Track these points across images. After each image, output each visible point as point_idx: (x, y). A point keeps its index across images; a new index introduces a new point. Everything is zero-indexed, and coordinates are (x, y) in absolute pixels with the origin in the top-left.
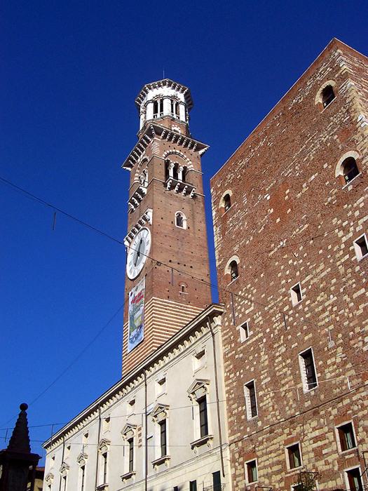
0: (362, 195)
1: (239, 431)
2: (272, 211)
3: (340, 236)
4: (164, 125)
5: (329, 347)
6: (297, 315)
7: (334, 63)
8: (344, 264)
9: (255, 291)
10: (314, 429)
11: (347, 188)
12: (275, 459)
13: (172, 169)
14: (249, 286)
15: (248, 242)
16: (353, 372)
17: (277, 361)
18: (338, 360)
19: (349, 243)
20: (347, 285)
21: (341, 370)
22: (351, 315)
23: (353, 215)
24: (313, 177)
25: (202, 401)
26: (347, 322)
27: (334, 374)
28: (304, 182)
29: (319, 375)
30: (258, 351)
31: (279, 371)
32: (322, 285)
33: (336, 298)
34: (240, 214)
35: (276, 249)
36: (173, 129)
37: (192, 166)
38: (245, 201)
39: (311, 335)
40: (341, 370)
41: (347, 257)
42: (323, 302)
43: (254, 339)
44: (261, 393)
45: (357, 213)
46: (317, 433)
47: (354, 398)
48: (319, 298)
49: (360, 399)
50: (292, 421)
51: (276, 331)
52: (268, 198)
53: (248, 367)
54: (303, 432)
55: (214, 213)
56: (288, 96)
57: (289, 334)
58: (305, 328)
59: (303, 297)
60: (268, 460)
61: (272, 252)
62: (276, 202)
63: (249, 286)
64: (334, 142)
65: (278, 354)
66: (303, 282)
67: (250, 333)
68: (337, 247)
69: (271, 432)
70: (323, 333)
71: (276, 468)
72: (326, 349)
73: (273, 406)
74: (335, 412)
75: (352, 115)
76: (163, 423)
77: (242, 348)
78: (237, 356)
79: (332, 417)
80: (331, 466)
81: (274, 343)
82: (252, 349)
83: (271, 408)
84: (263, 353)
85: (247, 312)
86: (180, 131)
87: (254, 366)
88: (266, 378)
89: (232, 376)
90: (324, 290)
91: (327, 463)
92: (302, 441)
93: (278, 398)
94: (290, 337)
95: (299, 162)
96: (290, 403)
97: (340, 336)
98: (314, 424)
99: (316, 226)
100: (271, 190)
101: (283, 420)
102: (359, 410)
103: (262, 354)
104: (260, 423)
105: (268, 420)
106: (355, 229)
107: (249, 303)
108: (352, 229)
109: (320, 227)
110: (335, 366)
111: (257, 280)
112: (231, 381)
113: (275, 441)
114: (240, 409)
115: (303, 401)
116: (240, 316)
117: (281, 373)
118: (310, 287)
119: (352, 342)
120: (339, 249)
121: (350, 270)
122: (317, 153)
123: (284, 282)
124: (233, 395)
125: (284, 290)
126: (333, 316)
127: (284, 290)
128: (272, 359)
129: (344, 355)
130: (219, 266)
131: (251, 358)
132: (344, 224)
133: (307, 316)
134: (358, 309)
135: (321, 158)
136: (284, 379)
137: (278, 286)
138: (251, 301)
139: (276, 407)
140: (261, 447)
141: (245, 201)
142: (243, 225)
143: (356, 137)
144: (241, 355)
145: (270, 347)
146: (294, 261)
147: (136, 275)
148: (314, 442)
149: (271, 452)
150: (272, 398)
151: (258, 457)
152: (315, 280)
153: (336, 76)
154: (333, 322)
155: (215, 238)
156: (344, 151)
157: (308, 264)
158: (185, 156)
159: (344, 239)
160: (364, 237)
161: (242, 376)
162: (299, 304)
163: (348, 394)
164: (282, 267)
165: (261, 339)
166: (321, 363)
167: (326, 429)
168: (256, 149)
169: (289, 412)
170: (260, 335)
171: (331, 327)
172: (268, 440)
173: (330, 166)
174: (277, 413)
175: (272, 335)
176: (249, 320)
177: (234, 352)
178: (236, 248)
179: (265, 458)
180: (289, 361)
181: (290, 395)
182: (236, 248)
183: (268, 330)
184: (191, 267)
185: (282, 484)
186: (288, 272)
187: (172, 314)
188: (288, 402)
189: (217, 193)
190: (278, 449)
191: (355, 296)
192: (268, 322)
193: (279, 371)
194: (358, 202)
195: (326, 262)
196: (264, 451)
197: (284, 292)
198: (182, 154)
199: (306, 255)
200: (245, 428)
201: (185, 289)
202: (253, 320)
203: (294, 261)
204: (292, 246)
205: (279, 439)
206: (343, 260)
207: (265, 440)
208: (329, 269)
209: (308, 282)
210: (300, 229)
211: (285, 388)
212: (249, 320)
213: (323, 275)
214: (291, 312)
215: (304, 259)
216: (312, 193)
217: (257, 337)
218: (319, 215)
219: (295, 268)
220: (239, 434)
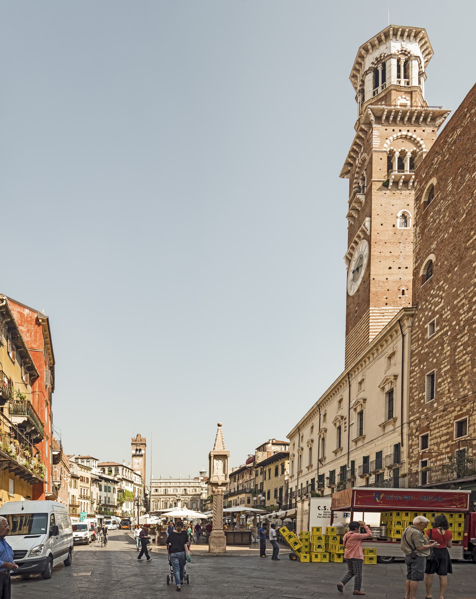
43: (440, 334)
84: (447, 344)
85: (436, 309)
93: (454, 382)
96: (465, 386)
101: (456, 400)
103: (445, 346)
113: (446, 418)
136: (462, 365)
139: (451, 390)
149: (442, 426)
170: (445, 329)
174: (452, 395)
176: (437, 316)
196: (437, 426)
202: (441, 315)
211: (462, 373)
217: (442, 332)
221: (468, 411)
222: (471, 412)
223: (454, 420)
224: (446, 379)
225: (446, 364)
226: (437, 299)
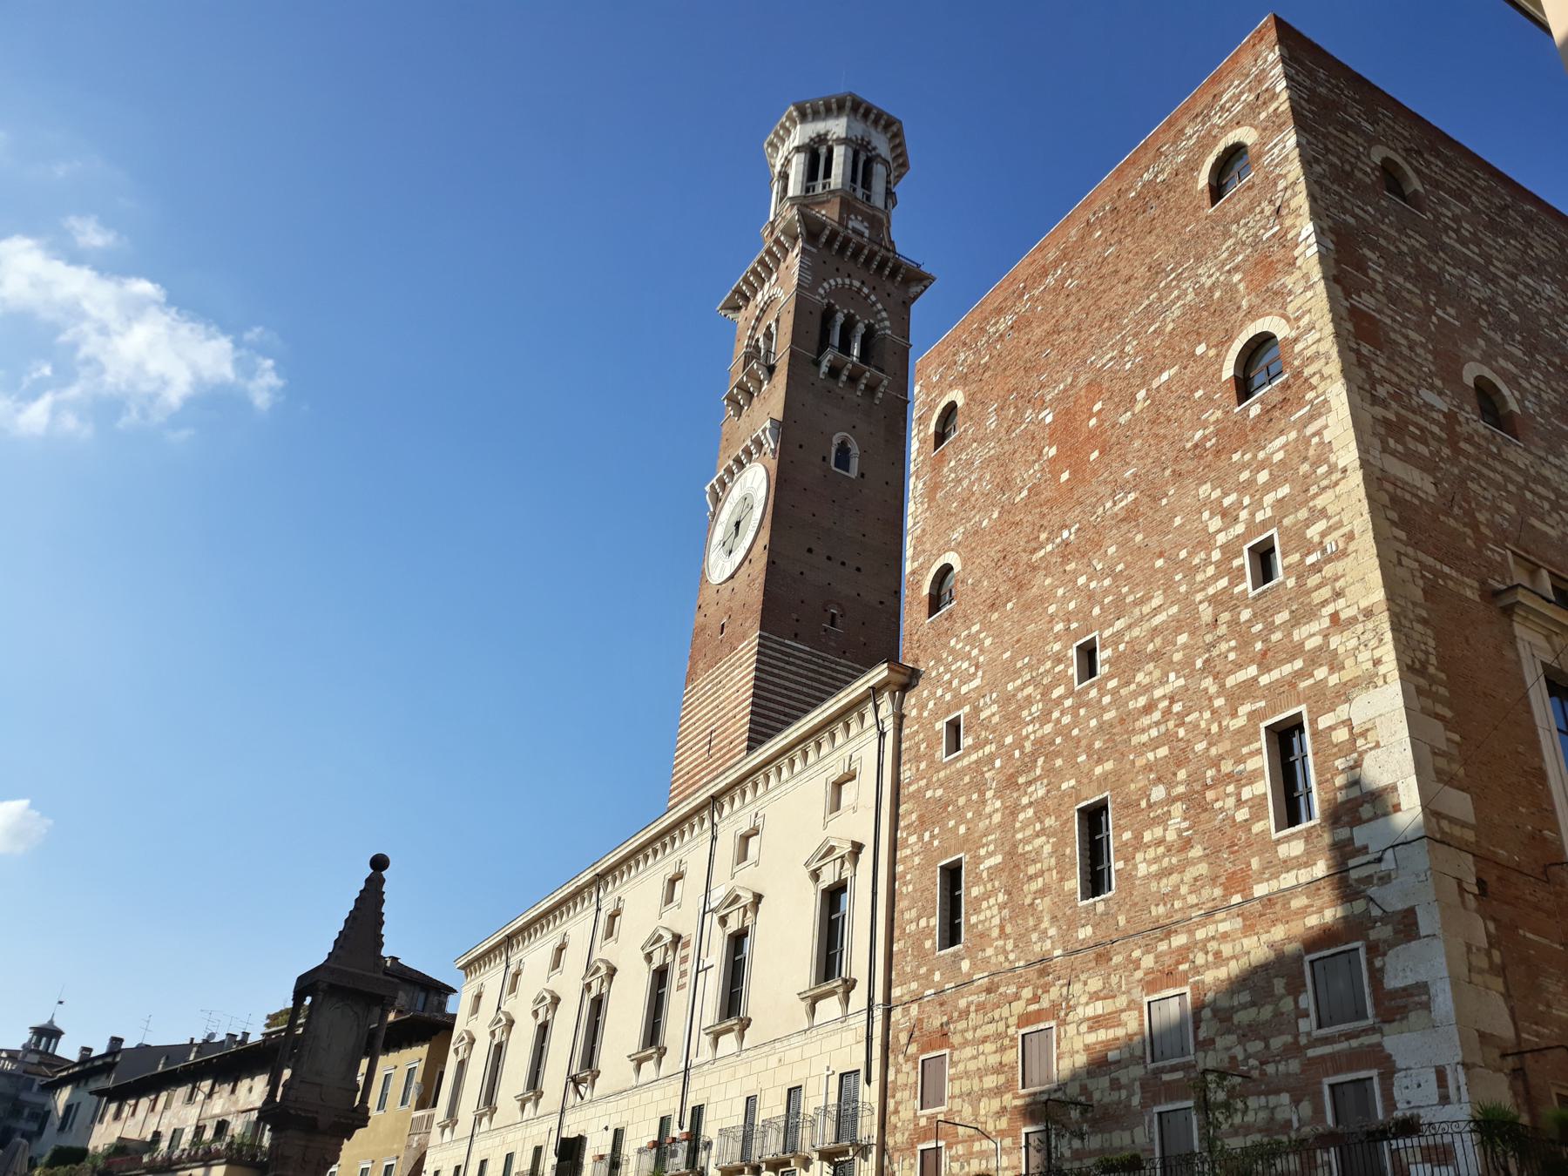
0: (1282, 432)
1: (916, 977)
2: (1053, 451)
3: (1211, 530)
4: (829, 213)
5: (1153, 798)
6: (1082, 712)
7: (1260, 82)
8: (1212, 600)
9: (988, 642)
10: (1095, 997)
11: (1247, 409)
12: (993, 1060)
13: (838, 329)
14: (975, 628)
15: (985, 523)
16: (1203, 868)
17: (1021, 817)
18: (1171, 836)
19: (1230, 551)
20: (1215, 652)
21: (1174, 860)
22: (1215, 728)
23: (1251, 482)
24: (1165, 376)
25: (833, 897)
26: (1204, 745)
27: (1154, 868)
28: (1140, 387)
29: (1120, 865)
30: (981, 787)
31: (1026, 841)
32: (1151, 647)
33: (1182, 682)
34: (979, 453)
35: (1049, 548)
36: (851, 224)
37: (887, 323)
38: (992, 423)
39: (1109, 766)
40: (1174, 860)
41: (1224, 582)
42: (1148, 689)
43: (974, 757)
44: (975, 891)
45: (1263, 477)
46: (1098, 1008)
47: (1200, 934)
48: (1140, 677)
49: (1213, 938)
50: (1043, 964)
51: (1028, 745)
52: (1049, 419)
53: (951, 823)
54: (1067, 1000)
55: (914, 445)
56: (1132, 163)
57: (1058, 754)
58: (1098, 745)
59: (1102, 670)
60: (975, 1058)
61: (1042, 553)
62: (1066, 430)
63: (975, 628)
64: (1232, 288)
65: (1025, 800)
66: (1107, 633)
67: (966, 742)
68: (1203, 555)
69: (989, 991)
70: (1140, 762)
71: (990, 1081)
72: (1143, 804)
73: (1002, 928)
74: (1148, 961)
75: (1288, 223)
76: (737, 941)
77: (942, 774)
78: (929, 794)
79: (1139, 974)
80: (1124, 1094)
81: (1019, 773)
82: (967, 779)
83: (995, 933)
85: (964, 689)
86: (867, 233)
87: (968, 822)
88: (990, 855)
89: (913, 839)
90: (1157, 656)
91: (1115, 1085)
92: (1063, 1023)
93: (1017, 910)
94: (1059, 762)
95: (1136, 335)
96: (1043, 926)
97: (1182, 775)
98: (1095, 984)
99: (1156, 500)
100: (1057, 399)
101: (1022, 963)
102: (1207, 966)
103: (989, 794)
104: (965, 965)
105: (986, 960)
106: (1253, 515)
107: (972, 670)
108: (1244, 515)
109: (1164, 501)
110: (1161, 850)
111: (996, 616)
112: (908, 852)
114: (923, 923)
115: (1073, 924)
116: (948, 697)
117: (1028, 848)
118: (1122, 647)
119: (1210, 795)
120: (1207, 562)
121: (1225, 617)
122: (1184, 314)
123: (1059, 627)
124: (910, 888)
125: (1057, 647)
126: (1171, 724)
127: (1057, 647)
128: (1013, 811)
129: (1185, 825)
130: (913, 573)
131: (962, 801)
132: (1227, 502)
133: (1107, 717)
134: (1234, 715)
135: (1193, 330)
137: (1042, 637)
138: (977, 667)
139: (1008, 929)
140: (961, 1025)
141: (992, 423)
142: (980, 479)
143: (1289, 281)
144: (939, 792)
145: (1010, 782)
146: (1090, 580)
147: (727, 574)
148: (1091, 1029)
150: (1002, 907)
151: (953, 1048)
152: (1136, 632)
153: (1263, 116)
154: (1168, 738)
155: (911, 508)
156: (1253, 314)
157: (1125, 590)
158: (873, 298)
159: (1221, 539)
160: (1271, 537)
161: (936, 843)
162: (1092, 685)
163: (1186, 924)
164: (1060, 592)
165: (990, 759)
166: (1127, 835)
167: (1122, 1001)
168: (1037, 293)
169: (1037, 948)
170: (987, 749)
171: (1163, 752)
172: (980, 1007)
173: (1212, 352)
174: (1010, 946)
175: (1017, 754)
176: (967, 709)
177: (923, 783)
178: (957, 535)
179: (969, 1051)
180: (1050, 822)
181: (1043, 904)
182: (957, 535)
183: (1009, 740)
184: (858, 569)
185: (1003, 1124)
186: (1072, 605)
187: (801, 676)
188: (1039, 920)
189: (928, 395)
190: (999, 1036)
191: (1231, 681)
192: (1012, 720)
193: (1026, 841)
194: (1271, 447)
195: (1169, 587)
197: (1058, 652)
198: (866, 290)
199: (1120, 567)
200: (931, 972)
201: (838, 621)
202: (976, 710)
203: (1090, 580)
204: (1090, 543)
205: (1005, 1011)
206: (1211, 591)
207: (973, 1008)
208: (1175, 609)
209: (1119, 635)
210: (1115, 504)
212: (967, 709)
213: (1157, 620)
214: (1068, 703)
215: (1116, 577)
216: (1157, 413)
217: (980, 753)
218: (1168, 472)
219: (1091, 597)
220: (914, 985)
221: (1055, 1006)
222: (1062, 1014)
223: (1019, 1026)
224: (994, 892)
225: (992, 847)
226: (965, 665)
